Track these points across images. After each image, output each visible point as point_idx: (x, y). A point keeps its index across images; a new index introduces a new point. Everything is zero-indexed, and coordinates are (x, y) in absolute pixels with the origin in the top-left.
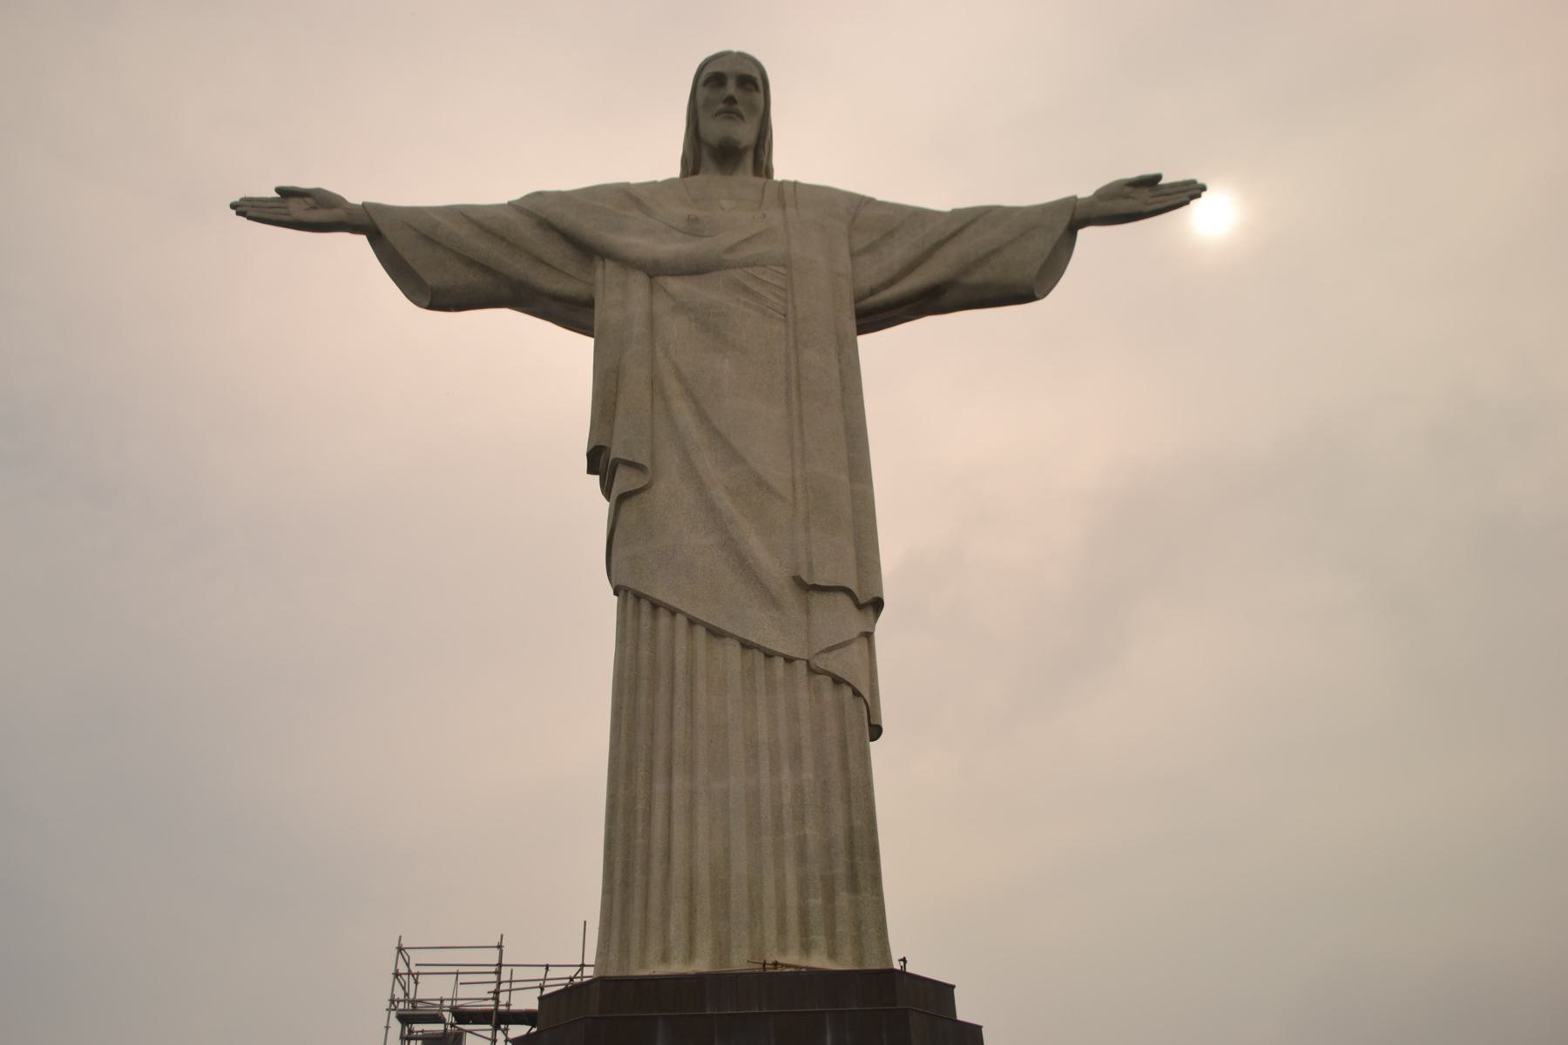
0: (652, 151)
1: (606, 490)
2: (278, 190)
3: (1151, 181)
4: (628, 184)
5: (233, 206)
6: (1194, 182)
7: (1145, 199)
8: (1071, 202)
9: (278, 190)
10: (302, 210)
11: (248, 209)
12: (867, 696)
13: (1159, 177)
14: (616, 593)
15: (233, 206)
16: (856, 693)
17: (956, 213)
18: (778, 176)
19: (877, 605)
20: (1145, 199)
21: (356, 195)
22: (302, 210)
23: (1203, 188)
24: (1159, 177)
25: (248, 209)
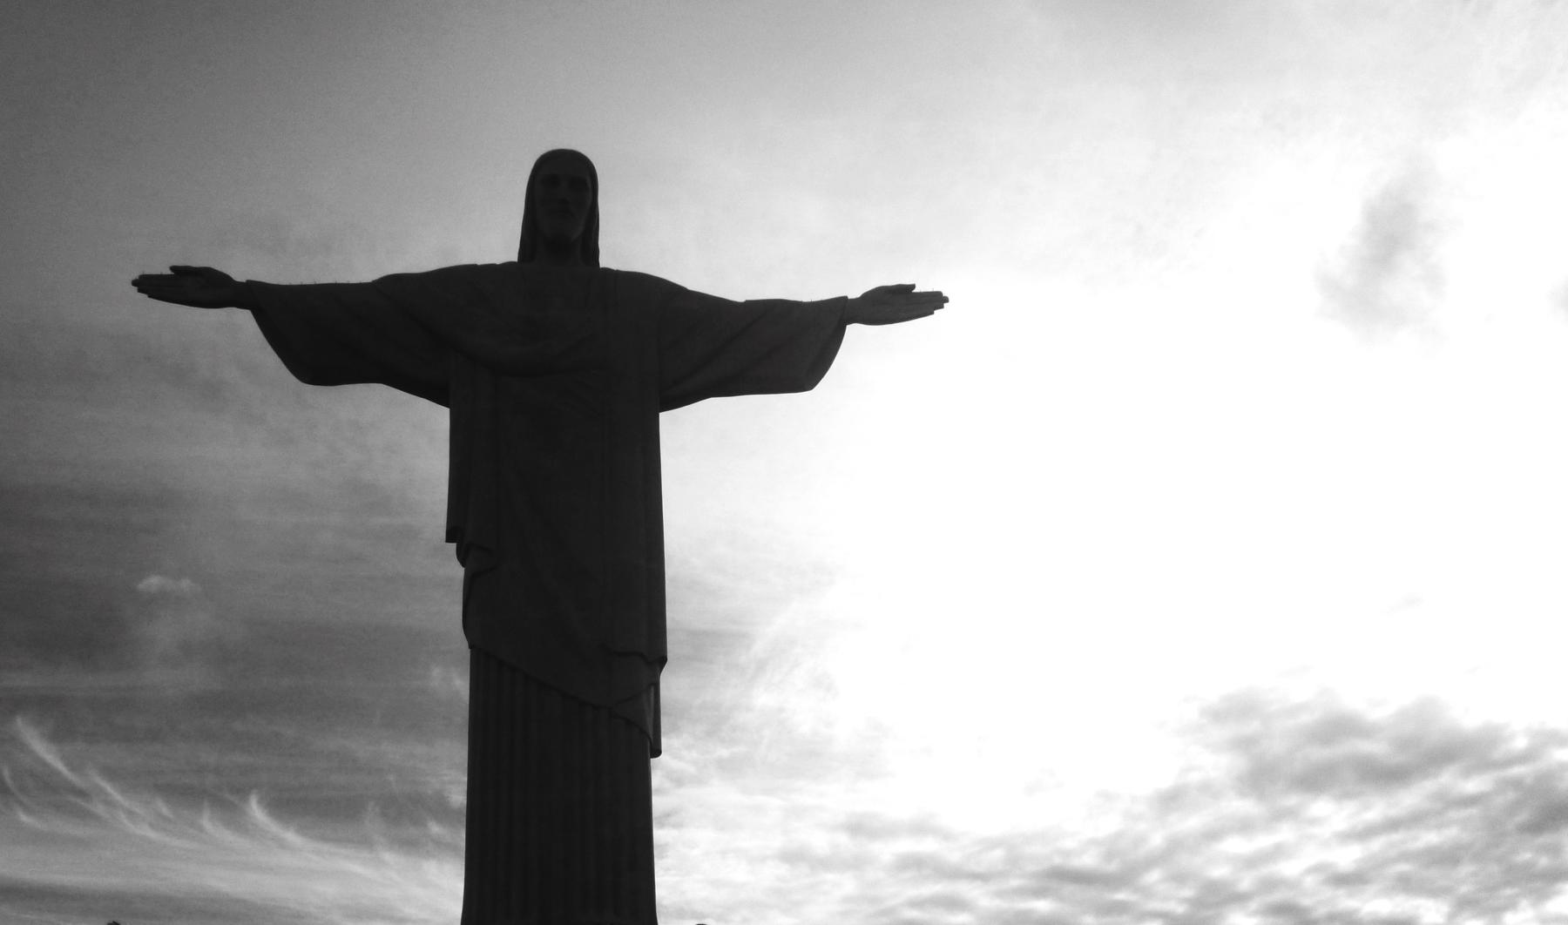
0: (493, 236)
1: (462, 557)
2: (173, 268)
3: (906, 290)
4: (475, 266)
5: (135, 283)
6: (939, 294)
7: (898, 304)
8: (843, 300)
9: (173, 268)
10: (194, 286)
11: (150, 286)
12: (651, 732)
13: (913, 286)
14: (471, 647)
15: (135, 283)
16: (643, 732)
17: (748, 303)
18: (606, 261)
19: (662, 660)
20: (898, 304)
21: (240, 271)
22: (194, 286)
23: (946, 300)
24: (913, 286)
25: (150, 286)
